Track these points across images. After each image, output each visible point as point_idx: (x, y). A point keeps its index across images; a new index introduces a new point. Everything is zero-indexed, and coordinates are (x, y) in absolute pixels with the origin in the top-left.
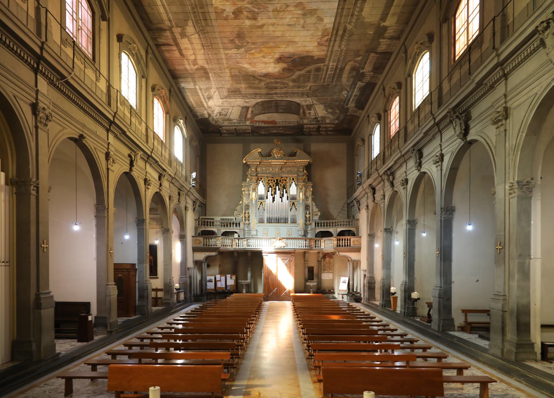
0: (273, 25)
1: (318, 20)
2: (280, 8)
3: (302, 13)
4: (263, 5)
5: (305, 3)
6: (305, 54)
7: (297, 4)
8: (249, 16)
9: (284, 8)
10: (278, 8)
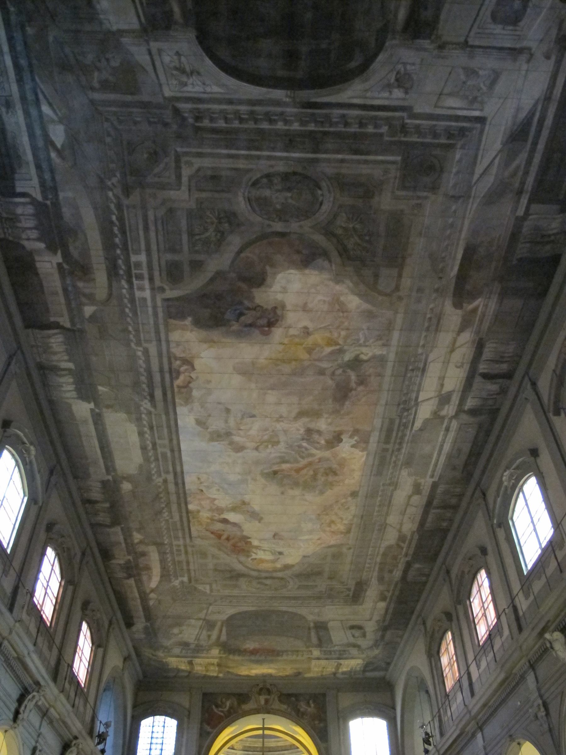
0: (280, 419)
1: (204, 424)
2: (267, 446)
3: (234, 437)
5: (230, 450)
6: (215, 334)
10: (270, 446)
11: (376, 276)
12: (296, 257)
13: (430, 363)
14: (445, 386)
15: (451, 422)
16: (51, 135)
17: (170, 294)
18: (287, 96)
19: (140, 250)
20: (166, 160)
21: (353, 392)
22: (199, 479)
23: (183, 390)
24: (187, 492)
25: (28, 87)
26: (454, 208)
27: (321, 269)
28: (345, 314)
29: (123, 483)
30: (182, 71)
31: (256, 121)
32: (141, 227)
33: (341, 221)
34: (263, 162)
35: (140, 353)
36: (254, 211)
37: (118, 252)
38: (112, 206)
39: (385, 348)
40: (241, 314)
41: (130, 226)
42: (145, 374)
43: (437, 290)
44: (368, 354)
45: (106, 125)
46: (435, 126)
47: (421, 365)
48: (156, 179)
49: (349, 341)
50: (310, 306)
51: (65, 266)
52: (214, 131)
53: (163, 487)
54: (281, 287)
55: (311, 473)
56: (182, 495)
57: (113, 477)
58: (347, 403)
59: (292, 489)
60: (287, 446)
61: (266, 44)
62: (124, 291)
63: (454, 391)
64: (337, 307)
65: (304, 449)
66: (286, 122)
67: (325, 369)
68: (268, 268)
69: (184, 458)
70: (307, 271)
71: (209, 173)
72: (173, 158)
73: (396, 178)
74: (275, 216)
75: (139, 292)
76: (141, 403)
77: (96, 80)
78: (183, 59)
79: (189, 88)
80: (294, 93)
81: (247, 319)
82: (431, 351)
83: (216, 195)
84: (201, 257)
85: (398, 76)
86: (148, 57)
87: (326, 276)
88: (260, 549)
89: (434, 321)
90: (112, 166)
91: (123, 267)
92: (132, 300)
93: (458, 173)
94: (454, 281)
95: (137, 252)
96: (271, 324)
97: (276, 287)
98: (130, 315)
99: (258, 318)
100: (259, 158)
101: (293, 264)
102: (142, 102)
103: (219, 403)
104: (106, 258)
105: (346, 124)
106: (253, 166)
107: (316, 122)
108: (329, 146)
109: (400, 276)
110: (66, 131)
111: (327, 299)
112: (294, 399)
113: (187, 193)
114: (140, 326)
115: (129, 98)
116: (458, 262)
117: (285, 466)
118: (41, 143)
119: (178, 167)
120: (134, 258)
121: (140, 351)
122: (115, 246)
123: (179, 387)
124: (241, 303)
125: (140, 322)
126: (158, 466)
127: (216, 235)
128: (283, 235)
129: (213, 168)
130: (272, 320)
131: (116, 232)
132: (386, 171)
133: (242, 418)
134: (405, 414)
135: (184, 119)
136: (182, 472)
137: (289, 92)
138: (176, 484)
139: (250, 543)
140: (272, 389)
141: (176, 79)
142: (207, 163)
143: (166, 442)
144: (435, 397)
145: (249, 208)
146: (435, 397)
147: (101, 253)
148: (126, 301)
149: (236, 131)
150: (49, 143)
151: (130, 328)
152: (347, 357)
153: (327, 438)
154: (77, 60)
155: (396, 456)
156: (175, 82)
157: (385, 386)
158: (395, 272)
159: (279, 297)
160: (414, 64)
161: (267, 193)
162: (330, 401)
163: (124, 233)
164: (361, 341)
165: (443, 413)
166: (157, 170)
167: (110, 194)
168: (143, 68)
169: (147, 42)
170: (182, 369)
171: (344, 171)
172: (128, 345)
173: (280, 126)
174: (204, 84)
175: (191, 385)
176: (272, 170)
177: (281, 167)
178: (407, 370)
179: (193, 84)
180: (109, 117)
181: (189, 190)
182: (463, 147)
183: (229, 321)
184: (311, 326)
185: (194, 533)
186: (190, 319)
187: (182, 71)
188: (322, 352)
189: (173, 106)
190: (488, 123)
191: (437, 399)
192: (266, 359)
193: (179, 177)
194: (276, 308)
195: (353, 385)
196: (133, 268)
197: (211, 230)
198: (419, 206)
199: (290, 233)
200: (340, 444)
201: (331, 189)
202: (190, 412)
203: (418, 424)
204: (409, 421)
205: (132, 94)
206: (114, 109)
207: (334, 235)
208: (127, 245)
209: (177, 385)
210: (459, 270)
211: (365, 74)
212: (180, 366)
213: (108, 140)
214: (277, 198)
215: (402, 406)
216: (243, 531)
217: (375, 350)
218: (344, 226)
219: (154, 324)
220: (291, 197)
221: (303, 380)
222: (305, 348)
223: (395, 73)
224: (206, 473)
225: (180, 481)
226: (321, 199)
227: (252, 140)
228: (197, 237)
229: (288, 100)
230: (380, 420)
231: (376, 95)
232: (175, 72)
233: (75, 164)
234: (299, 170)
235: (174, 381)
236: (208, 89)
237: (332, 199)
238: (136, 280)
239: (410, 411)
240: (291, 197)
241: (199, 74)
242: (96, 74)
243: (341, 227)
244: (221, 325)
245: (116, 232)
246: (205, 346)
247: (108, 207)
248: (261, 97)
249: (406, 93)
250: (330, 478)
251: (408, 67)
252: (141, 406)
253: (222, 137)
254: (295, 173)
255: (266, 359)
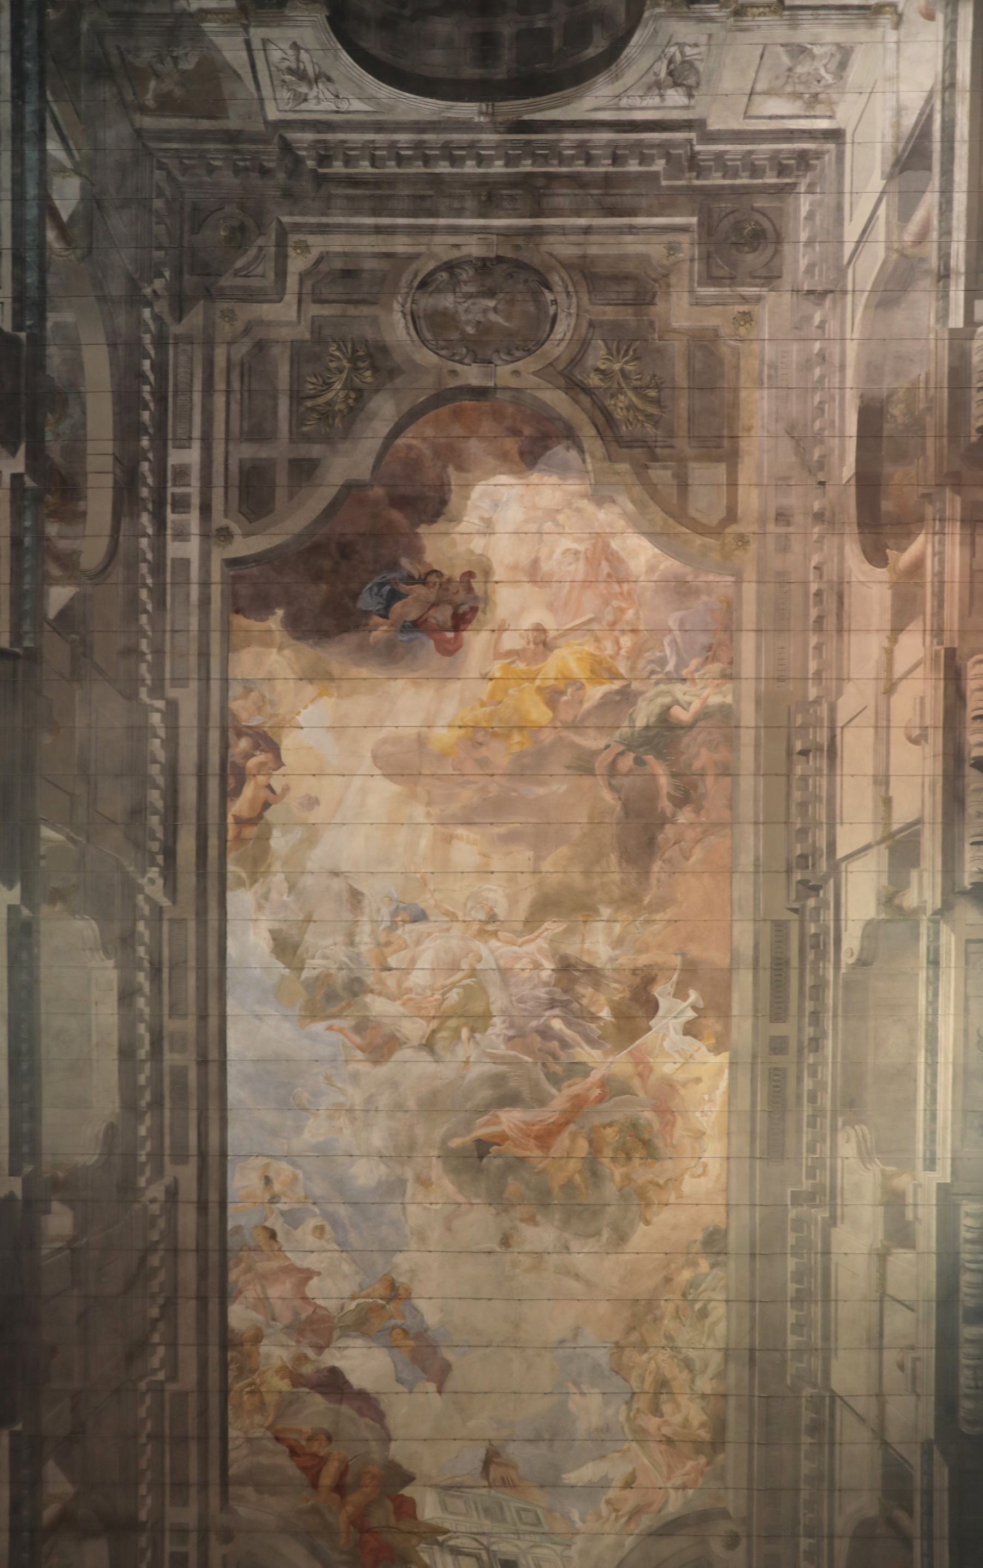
1: (296, 947)
3: (369, 998)
4: (529, 1052)
5: (360, 1055)
7: (391, 1053)
8: (590, 990)
9: (444, 1034)
10: (465, 1033)
11: (683, 486)
12: (511, 445)
13: (842, 728)
14: (895, 805)
15: (937, 934)
16: (54, 196)
17: (242, 547)
18: (481, 113)
19: (190, 438)
20: (260, 241)
21: (669, 831)
22: (268, 1181)
23: (250, 832)
24: (232, 1242)
25: (30, 108)
26: (817, 318)
27: (563, 470)
28: (626, 587)
29: (48, 1211)
30: (301, 75)
31: (427, 160)
32: (198, 386)
33: (598, 356)
34: (438, 239)
35: (156, 718)
36: (424, 342)
37: (145, 442)
38: (147, 338)
39: (728, 686)
40: (395, 596)
41: (176, 385)
42: (161, 781)
43: (819, 517)
44: (690, 704)
45: (158, 175)
46: (751, 152)
47: (823, 737)
48: (240, 281)
49: (641, 664)
50: (545, 567)
51: (29, 482)
52: (354, 182)
53: (162, 1223)
54: (482, 519)
55: (583, 1146)
56: (214, 1258)
57: (27, 1183)
58: (657, 866)
59: (531, 1220)
60: (511, 1033)
61: (443, 27)
62: (144, 542)
63: (919, 821)
64: (605, 568)
65: (555, 1044)
66: (480, 160)
67: (596, 753)
68: (451, 470)
69: (235, 1092)
70: (534, 477)
71: (338, 264)
72: (273, 236)
73: (692, 260)
74: (464, 350)
75: (177, 544)
76: (140, 881)
77: (149, 96)
78: (304, 55)
79: (311, 105)
80: (493, 105)
81: (406, 609)
82: (840, 693)
83: (352, 311)
84: (316, 450)
85: (672, 67)
86: (244, 54)
87: (574, 486)
88: (441, 1545)
89: (830, 603)
90: (158, 254)
91: (150, 481)
92: (158, 568)
93: (810, 243)
94: (852, 490)
95: (185, 443)
96: (460, 621)
97: (471, 520)
98: (149, 607)
99: (434, 605)
100: (432, 230)
101: (505, 461)
102: (226, 132)
103: (336, 874)
104: (116, 459)
105: (589, 160)
106: (423, 249)
107: (534, 157)
108: (561, 202)
109: (733, 484)
110: (83, 188)
111: (581, 548)
112: (523, 856)
113: (295, 307)
114: (168, 636)
115: (205, 124)
116: (852, 445)
117: (510, 1119)
118: (32, 212)
119: (282, 259)
120: (175, 457)
121: (158, 710)
122: (138, 429)
123: (240, 821)
124: (394, 565)
125: (168, 628)
126: (157, 1132)
127: (347, 397)
128: (480, 393)
129: (345, 254)
130: (465, 608)
131: (148, 397)
132: (672, 249)
133: (393, 926)
134: (811, 902)
135: (299, 161)
136: (223, 1155)
137: (484, 106)
138: (202, 1207)
139: (412, 1503)
140: (469, 823)
141: (289, 90)
142: (337, 244)
143: (190, 1025)
144: (879, 843)
145: (415, 337)
146: (879, 843)
147: (109, 447)
148: (144, 568)
149: (391, 181)
150: (48, 208)
151: (144, 645)
152: (644, 714)
153: (617, 998)
154: (123, 60)
155: (814, 1074)
156: (286, 95)
157: (746, 809)
158: (721, 470)
159: (478, 545)
160: (696, 45)
161: (447, 301)
162: (613, 858)
163: (161, 399)
164: (670, 667)
165: (910, 899)
166: (239, 264)
167: (147, 313)
168: (235, 72)
169: (246, 28)
170: (252, 763)
171: (593, 250)
172: (132, 696)
173: (470, 168)
174: (337, 97)
175: (268, 814)
176: (455, 254)
177: (473, 248)
178: (789, 753)
179: (317, 98)
180: (165, 161)
181: (300, 302)
182: (810, 190)
183: (367, 614)
184: (550, 623)
185: (239, 1458)
186: (280, 612)
187: (301, 75)
188: (581, 702)
189: (281, 137)
190: (848, 139)
191: (883, 850)
192: (450, 726)
193: (281, 274)
194: (470, 574)
195: (665, 804)
196: (169, 484)
197: (338, 386)
198: (747, 318)
199: (495, 388)
200: (652, 1023)
201: (571, 289)
202: (260, 908)
203: (852, 941)
204: (827, 933)
205: (211, 117)
206: (175, 146)
207: (587, 391)
208: (166, 426)
209: (235, 817)
210: (859, 460)
211: (613, 67)
212: (248, 756)
213: (158, 204)
214: (467, 311)
215: (798, 876)
216: (390, 1440)
217: (706, 692)
218: (603, 367)
219: (200, 631)
220: (495, 310)
221: (541, 791)
222: (540, 690)
223: (666, 62)
224: (288, 1157)
225: (213, 1196)
226: (552, 310)
227: (423, 197)
228: (309, 403)
229: (482, 119)
230: (749, 927)
231: (638, 102)
232: (288, 78)
233: (90, 249)
234: (508, 253)
235: (229, 804)
236: (344, 106)
237: (573, 310)
238: (173, 512)
239: (821, 893)
240: (495, 310)
241: (329, 79)
242: (152, 84)
243: (597, 370)
244: (347, 630)
245: (148, 397)
246: (310, 690)
247: (139, 342)
248: (435, 118)
249: (690, 96)
250: (642, 1174)
251: (688, 51)
252: (141, 889)
253: (367, 192)
254: (500, 259)
255: (450, 726)
